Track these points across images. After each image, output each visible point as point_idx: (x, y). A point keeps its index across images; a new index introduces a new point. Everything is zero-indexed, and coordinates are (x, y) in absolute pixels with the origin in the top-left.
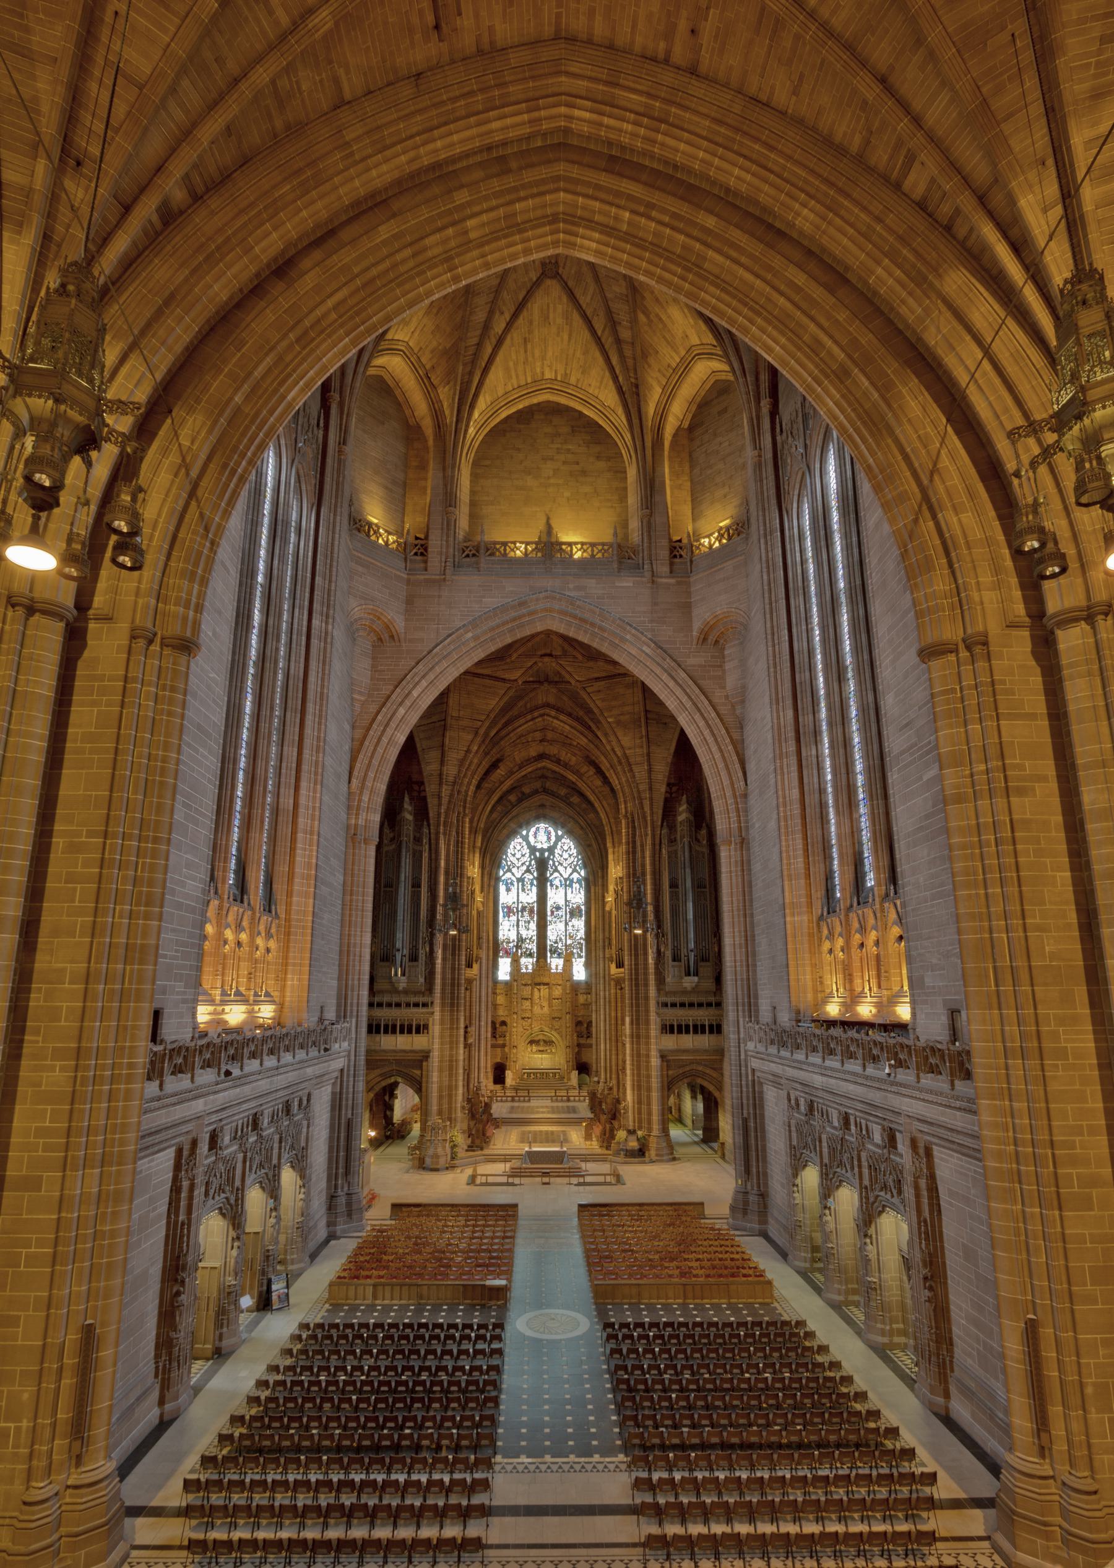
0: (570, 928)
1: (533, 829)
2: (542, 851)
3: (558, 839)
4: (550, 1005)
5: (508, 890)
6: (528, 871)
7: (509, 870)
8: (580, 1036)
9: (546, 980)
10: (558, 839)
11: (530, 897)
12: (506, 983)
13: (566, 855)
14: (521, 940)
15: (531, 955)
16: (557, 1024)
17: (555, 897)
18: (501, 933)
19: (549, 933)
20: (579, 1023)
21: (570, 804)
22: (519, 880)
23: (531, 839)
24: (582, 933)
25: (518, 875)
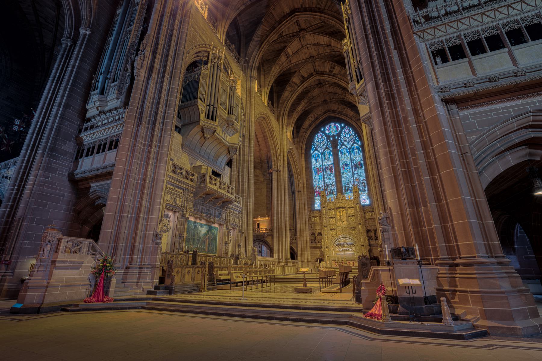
0: (355, 175)
1: (327, 127)
2: (334, 136)
3: (342, 128)
4: (348, 221)
5: (316, 160)
6: (327, 148)
7: (316, 150)
8: (370, 239)
9: (343, 205)
10: (342, 128)
11: (329, 162)
12: (320, 210)
13: (348, 136)
14: (326, 185)
15: (332, 193)
16: (353, 232)
17: (344, 159)
18: (314, 183)
19: (343, 179)
20: (368, 231)
21: (334, 75)
22: (322, 154)
23: (327, 132)
24: (364, 177)
25: (321, 151)
